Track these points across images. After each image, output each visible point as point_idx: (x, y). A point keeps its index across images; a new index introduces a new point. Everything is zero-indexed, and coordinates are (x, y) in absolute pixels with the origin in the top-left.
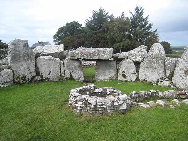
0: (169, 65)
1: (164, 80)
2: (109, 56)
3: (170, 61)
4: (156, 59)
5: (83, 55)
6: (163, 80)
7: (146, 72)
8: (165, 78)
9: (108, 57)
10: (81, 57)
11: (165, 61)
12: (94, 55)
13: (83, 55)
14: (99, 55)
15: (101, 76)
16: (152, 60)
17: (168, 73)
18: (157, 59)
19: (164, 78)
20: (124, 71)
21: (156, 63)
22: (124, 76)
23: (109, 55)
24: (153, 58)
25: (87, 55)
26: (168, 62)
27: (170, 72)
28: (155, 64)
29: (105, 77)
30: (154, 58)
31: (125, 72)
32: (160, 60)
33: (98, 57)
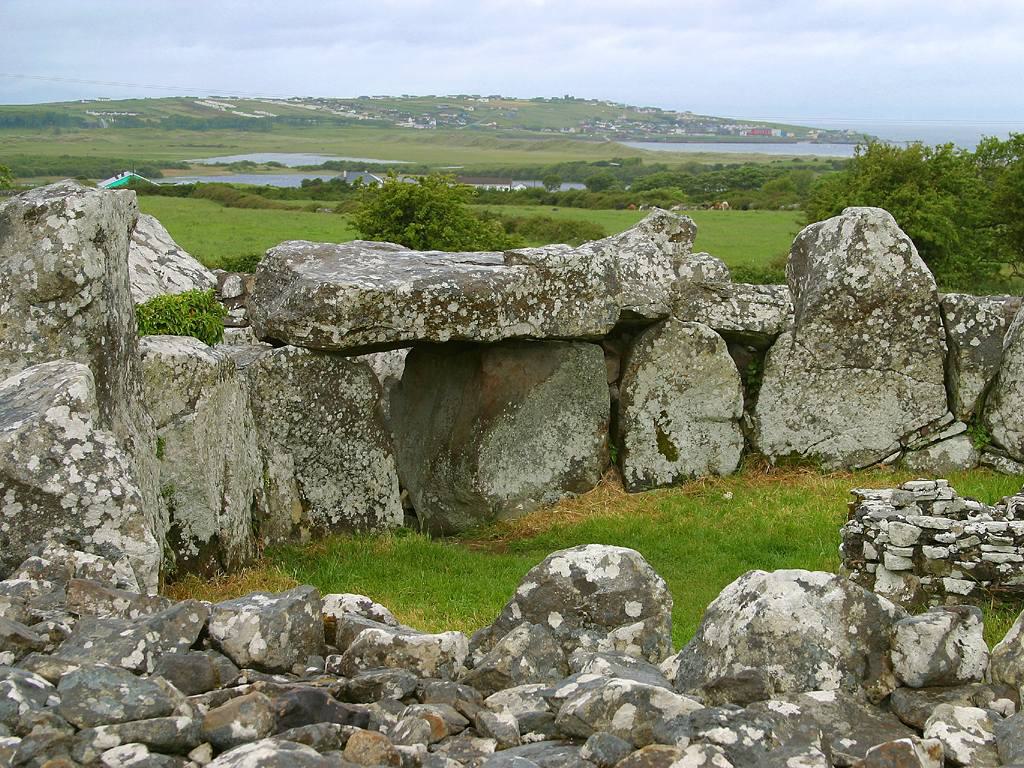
0: (975, 342)
1: (943, 435)
2: (608, 306)
3: (980, 318)
4: (889, 312)
5: (453, 307)
7: (814, 398)
8: (953, 422)
9: (605, 315)
10: (437, 327)
11: (951, 317)
12: (520, 308)
13: (453, 307)
14: (550, 307)
15: (501, 474)
17: (971, 386)
18: (896, 311)
19: (941, 423)
20: (664, 414)
21: (890, 337)
22: (667, 449)
23: (610, 299)
24: (873, 307)
25: (487, 311)
26: (972, 322)
27: (982, 383)
28: (885, 344)
29: (532, 479)
30: (881, 302)
31: (669, 422)
32: (919, 311)
33: (542, 319)
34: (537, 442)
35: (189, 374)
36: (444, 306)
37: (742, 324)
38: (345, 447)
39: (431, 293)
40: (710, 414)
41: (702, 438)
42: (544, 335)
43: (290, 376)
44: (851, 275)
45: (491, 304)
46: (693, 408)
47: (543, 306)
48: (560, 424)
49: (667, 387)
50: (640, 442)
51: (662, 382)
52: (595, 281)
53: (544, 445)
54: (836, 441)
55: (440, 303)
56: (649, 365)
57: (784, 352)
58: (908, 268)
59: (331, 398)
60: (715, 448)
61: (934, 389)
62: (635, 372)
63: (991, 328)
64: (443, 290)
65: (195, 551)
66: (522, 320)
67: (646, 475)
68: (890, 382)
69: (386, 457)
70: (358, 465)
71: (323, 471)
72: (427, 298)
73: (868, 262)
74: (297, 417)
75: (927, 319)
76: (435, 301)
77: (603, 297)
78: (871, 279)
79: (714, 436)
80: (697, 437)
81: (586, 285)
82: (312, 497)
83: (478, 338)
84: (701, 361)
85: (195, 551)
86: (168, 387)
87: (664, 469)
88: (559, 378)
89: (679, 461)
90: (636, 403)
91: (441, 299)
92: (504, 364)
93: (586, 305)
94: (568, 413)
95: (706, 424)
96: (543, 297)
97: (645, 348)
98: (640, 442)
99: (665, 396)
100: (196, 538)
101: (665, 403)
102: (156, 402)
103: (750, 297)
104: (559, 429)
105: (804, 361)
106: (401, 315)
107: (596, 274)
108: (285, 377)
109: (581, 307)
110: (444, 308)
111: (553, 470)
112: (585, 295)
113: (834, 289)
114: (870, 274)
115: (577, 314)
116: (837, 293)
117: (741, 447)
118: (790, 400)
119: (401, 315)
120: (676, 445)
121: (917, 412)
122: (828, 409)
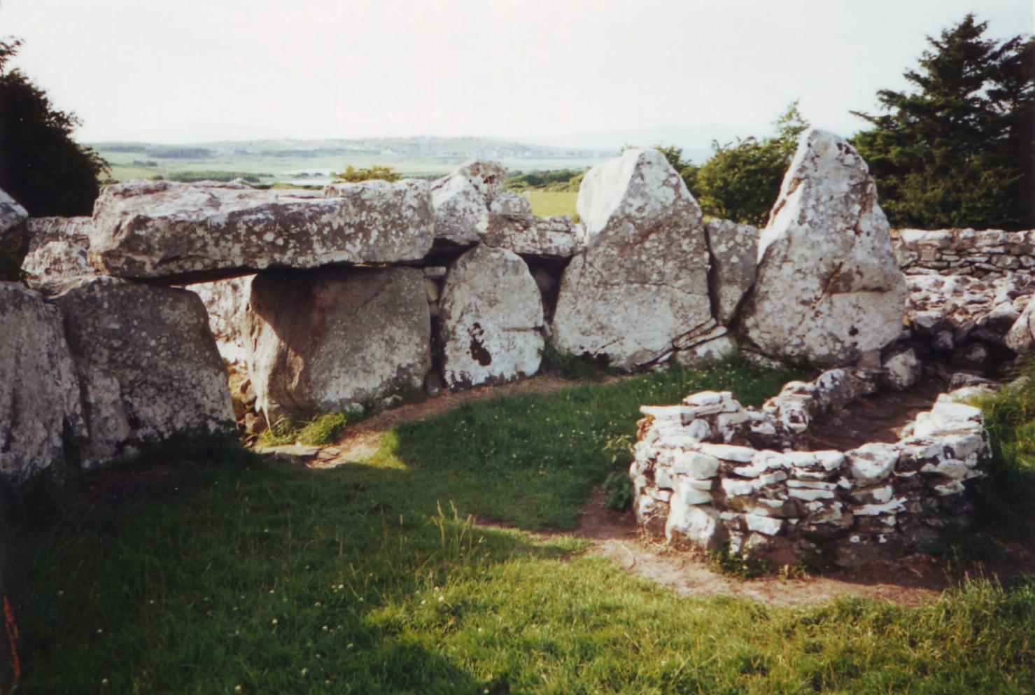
0: (735, 259)
1: (707, 337)
2: (422, 235)
3: (739, 239)
4: (663, 236)
5: (269, 237)
6: (700, 339)
7: (601, 308)
8: (714, 328)
10: (254, 256)
12: (338, 237)
14: (367, 235)
15: (334, 382)
16: (641, 242)
17: (731, 295)
18: (668, 236)
20: (477, 325)
21: (664, 257)
22: (482, 356)
23: (423, 228)
24: (650, 232)
26: (731, 243)
28: (659, 263)
29: (363, 385)
30: (657, 227)
31: (481, 333)
33: (359, 247)
36: (260, 235)
37: (541, 249)
38: (173, 368)
39: (245, 223)
43: (106, 305)
44: (631, 206)
47: (360, 235)
48: (386, 337)
49: (479, 303)
51: (474, 299)
52: (409, 213)
53: (373, 355)
57: (577, 272)
60: (521, 353)
64: (258, 221)
67: (463, 376)
68: (664, 294)
69: (217, 375)
71: (151, 391)
72: (242, 229)
74: (116, 343)
75: (694, 241)
76: (250, 231)
78: (648, 208)
81: (401, 217)
82: (142, 415)
83: (295, 266)
91: (257, 229)
95: (512, 334)
104: (387, 342)
105: (594, 279)
106: (217, 244)
107: (410, 207)
108: (100, 306)
109: (397, 235)
112: (400, 225)
115: (393, 243)
118: (582, 311)
119: (217, 244)
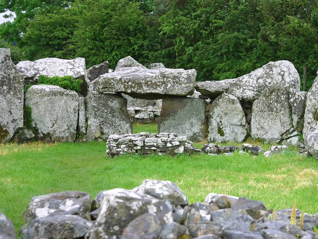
1: (292, 135)
2: (187, 87)
3: (297, 97)
4: (276, 94)
5: (130, 83)
6: (289, 136)
7: (262, 121)
8: (293, 131)
9: (185, 89)
10: (127, 89)
11: (290, 96)
12: (156, 85)
13: (130, 83)
14: (166, 85)
16: (270, 96)
18: (277, 93)
19: (291, 131)
20: (221, 122)
21: (277, 102)
23: (188, 85)
25: (140, 85)
27: (297, 118)
31: (222, 124)
32: (283, 94)
34: (184, 126)
35: (42, 93)
36: (128, 83)
37: (242, 96)
38: (113, 119)
39: (124, 79)
40: (234, 123)
41: (233, 131)
42: (163, 93)
43: (93, 99)
44: (267, 82)
45: (140, 83)
46: (230, 121)
47: (164, 85)
48: (191, 122)
49: (222, 114)
50: (212, 129)
51: (221, 112)
52: (183, 79)
53: (186, 128)
54: (267, 135)
55: (126, 82)
56: (218, 107)
57: (255, 105)
58: (282, 80)
59: (106, 106)
60: (236, 134)
61: (286, 119)
62: (213, 108)
63: (299, 100)
64: (127, 79)
65: (42, 136)
66: (154, 89)
67: (214, 139)
68: (278, 117)
69: (126, 124)
70: (116, 124)
71: (109, 125)
72: (123, 81)
73: (272, 77)
74: (96, 110)
75: (285, 96)
76: (125, 82)
77: (185, 84)
78: (272, 83)
79: (236, 130)
80: (232, 130)
81: (180, 80)
82: (105, 132)
83: (137, 92)
84: (230, 106)
85: (42, 136)
86: (35, 96)
87: (219, 138)
88: (187, 108)
89: (224, 136)
90: (214, 118)
91: (127, 81)
92: (167, 102)
93: (179, 86)
94: (193, 119)
95: (234, 126)
96: (164, 83)
97: (216, 101)
98: (212, 129)
99: (221, 116)
100: (42, 132)
101: (221, 118)
102: (32, 99)
103: (247, 88)
104: (190, 123)
105: (260, 108)
106: (117, 85)
107: (183, 77)
108: (92, 99)
109: (177, 86)
110: (128, 83)
111: (188, 135)
112: (179, 83)
113: (263, 86)
114: (272, 81)
115: (176, 88)
116: (264, 87)
117: (245, 134)
118: (257, 121)
119: (117, 85)
120: (224, 131)
121: (284, 127)
122: (265, 124)
